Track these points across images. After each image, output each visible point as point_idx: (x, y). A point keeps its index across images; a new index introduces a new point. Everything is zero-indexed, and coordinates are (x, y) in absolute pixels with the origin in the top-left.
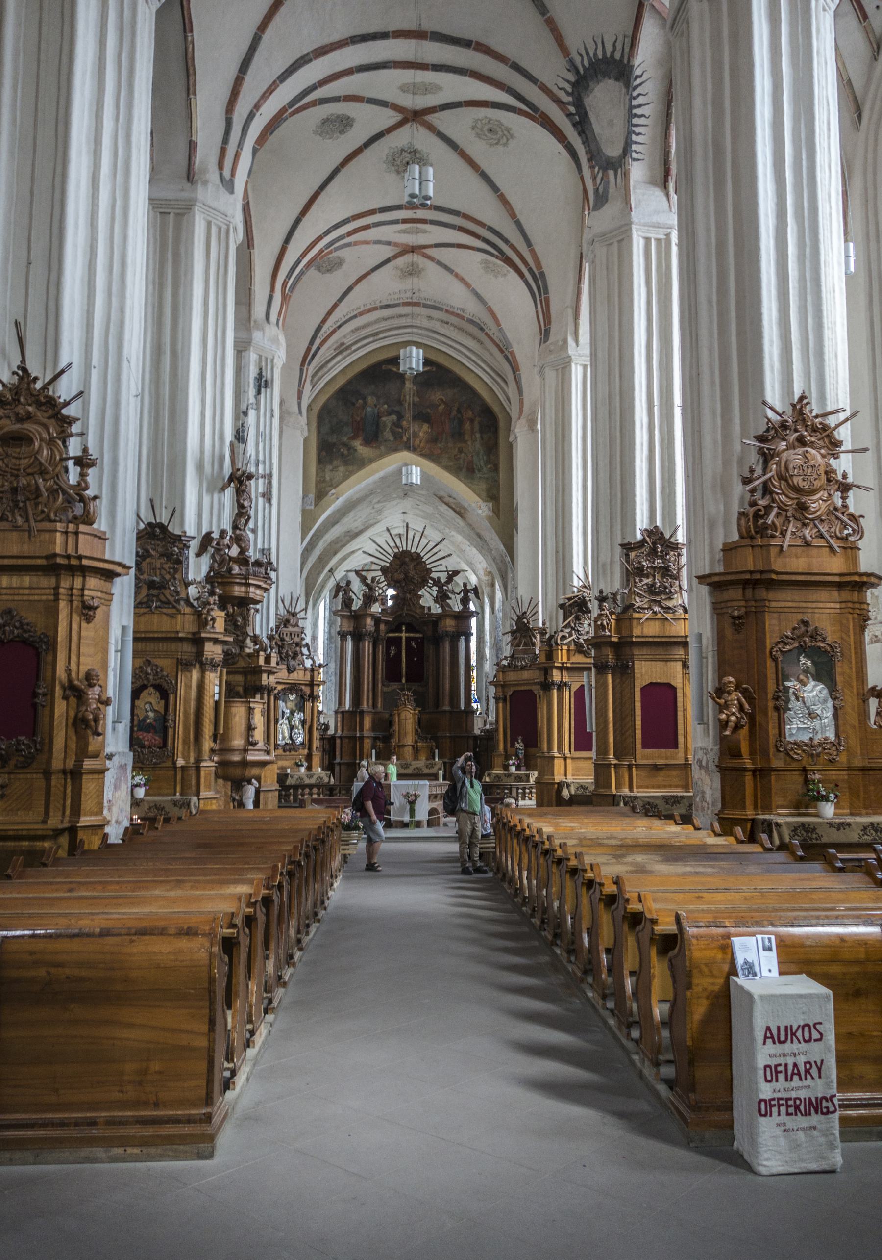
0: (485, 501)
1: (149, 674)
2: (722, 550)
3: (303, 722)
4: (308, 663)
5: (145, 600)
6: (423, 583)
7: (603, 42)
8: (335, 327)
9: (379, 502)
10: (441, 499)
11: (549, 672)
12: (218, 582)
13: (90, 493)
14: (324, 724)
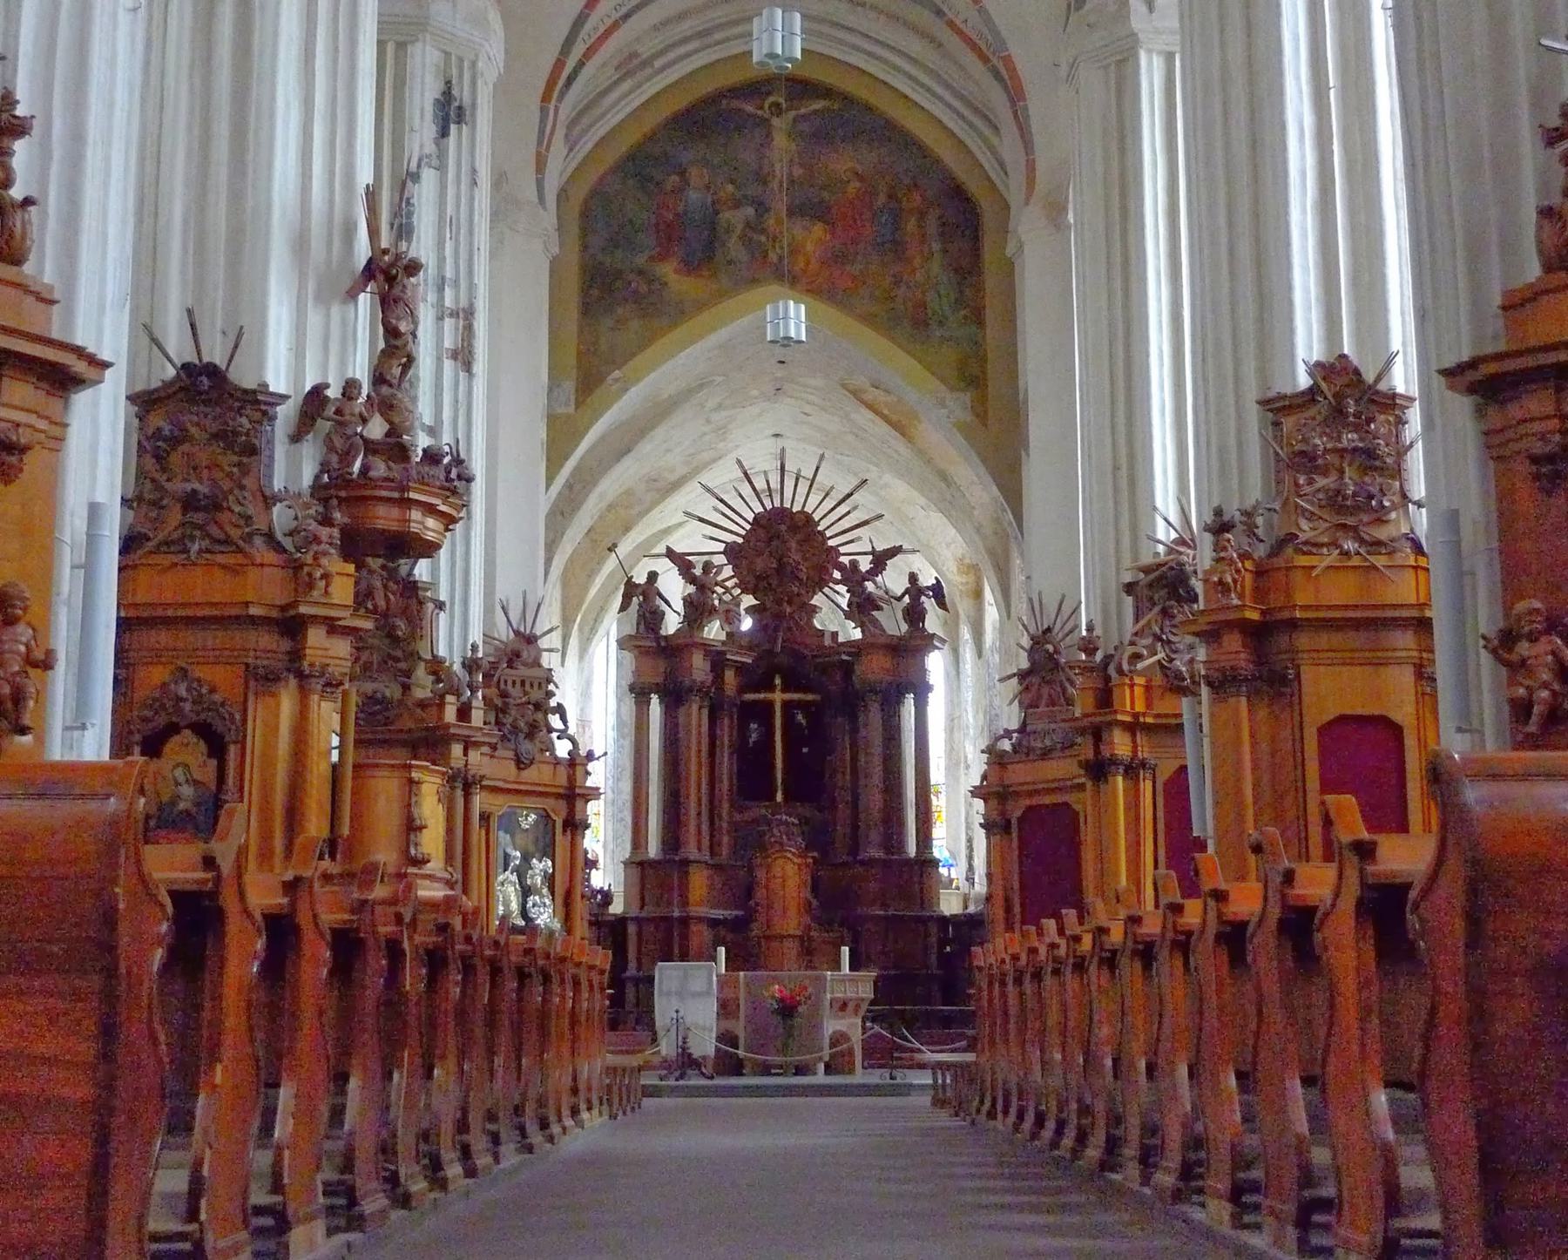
0: (952, 389)
1: (185, 700)
2: (1504, 308)
3: (550, 880)
4: (562, 749)
5: (175, 536)
6: (820, 581)
8: (616, 16)
9: (719, 407)
10: (856, 394)
11: (1105, 736)
12: (341, 500)
13: (16, 193)
14: (601, 891)
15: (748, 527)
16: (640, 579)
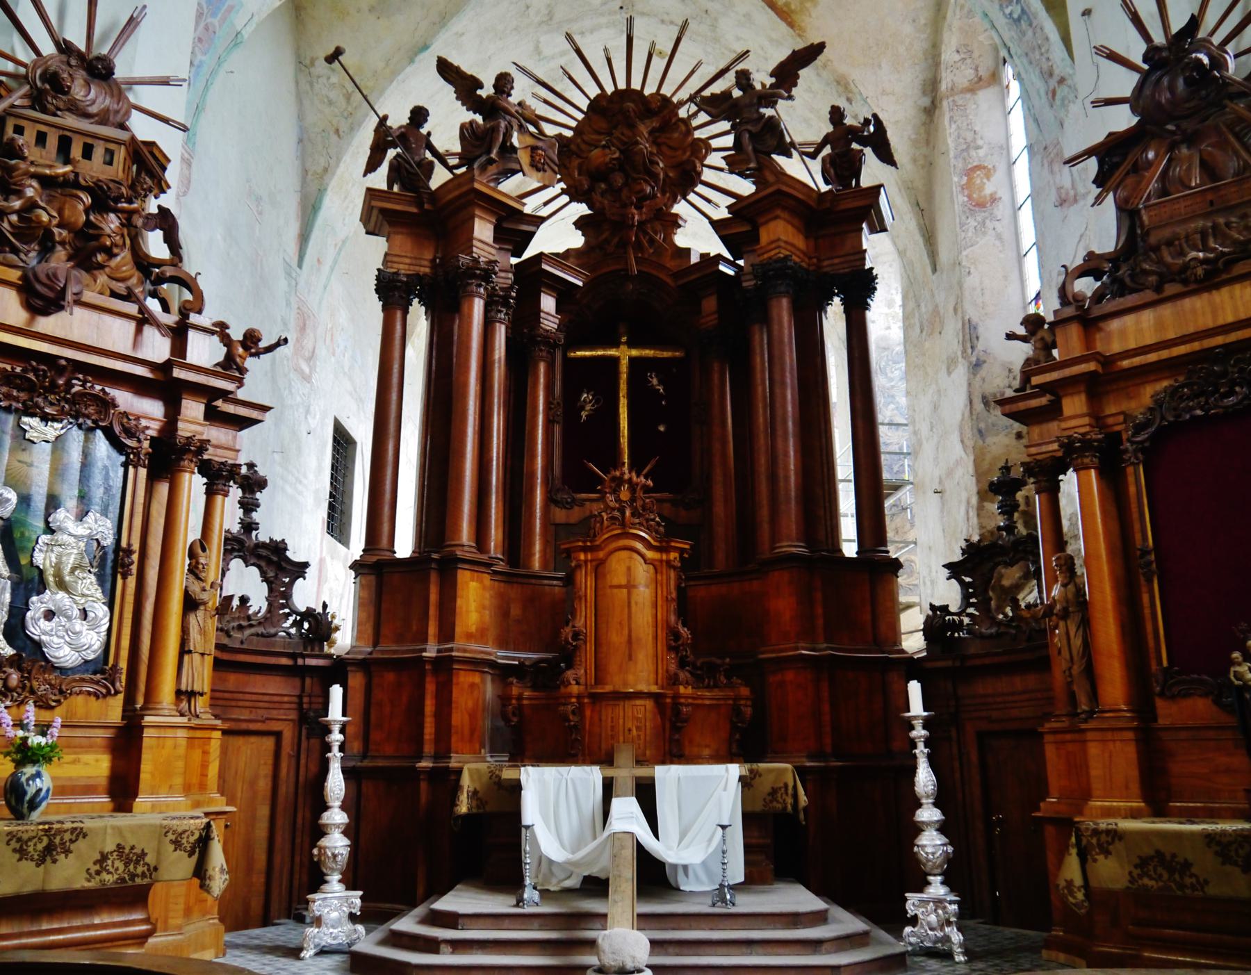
14: (309, 614)
15: (580, 116)
16: (399, 119)
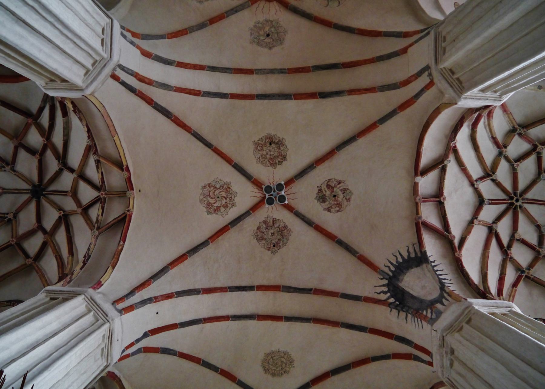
7: (400, 254)
